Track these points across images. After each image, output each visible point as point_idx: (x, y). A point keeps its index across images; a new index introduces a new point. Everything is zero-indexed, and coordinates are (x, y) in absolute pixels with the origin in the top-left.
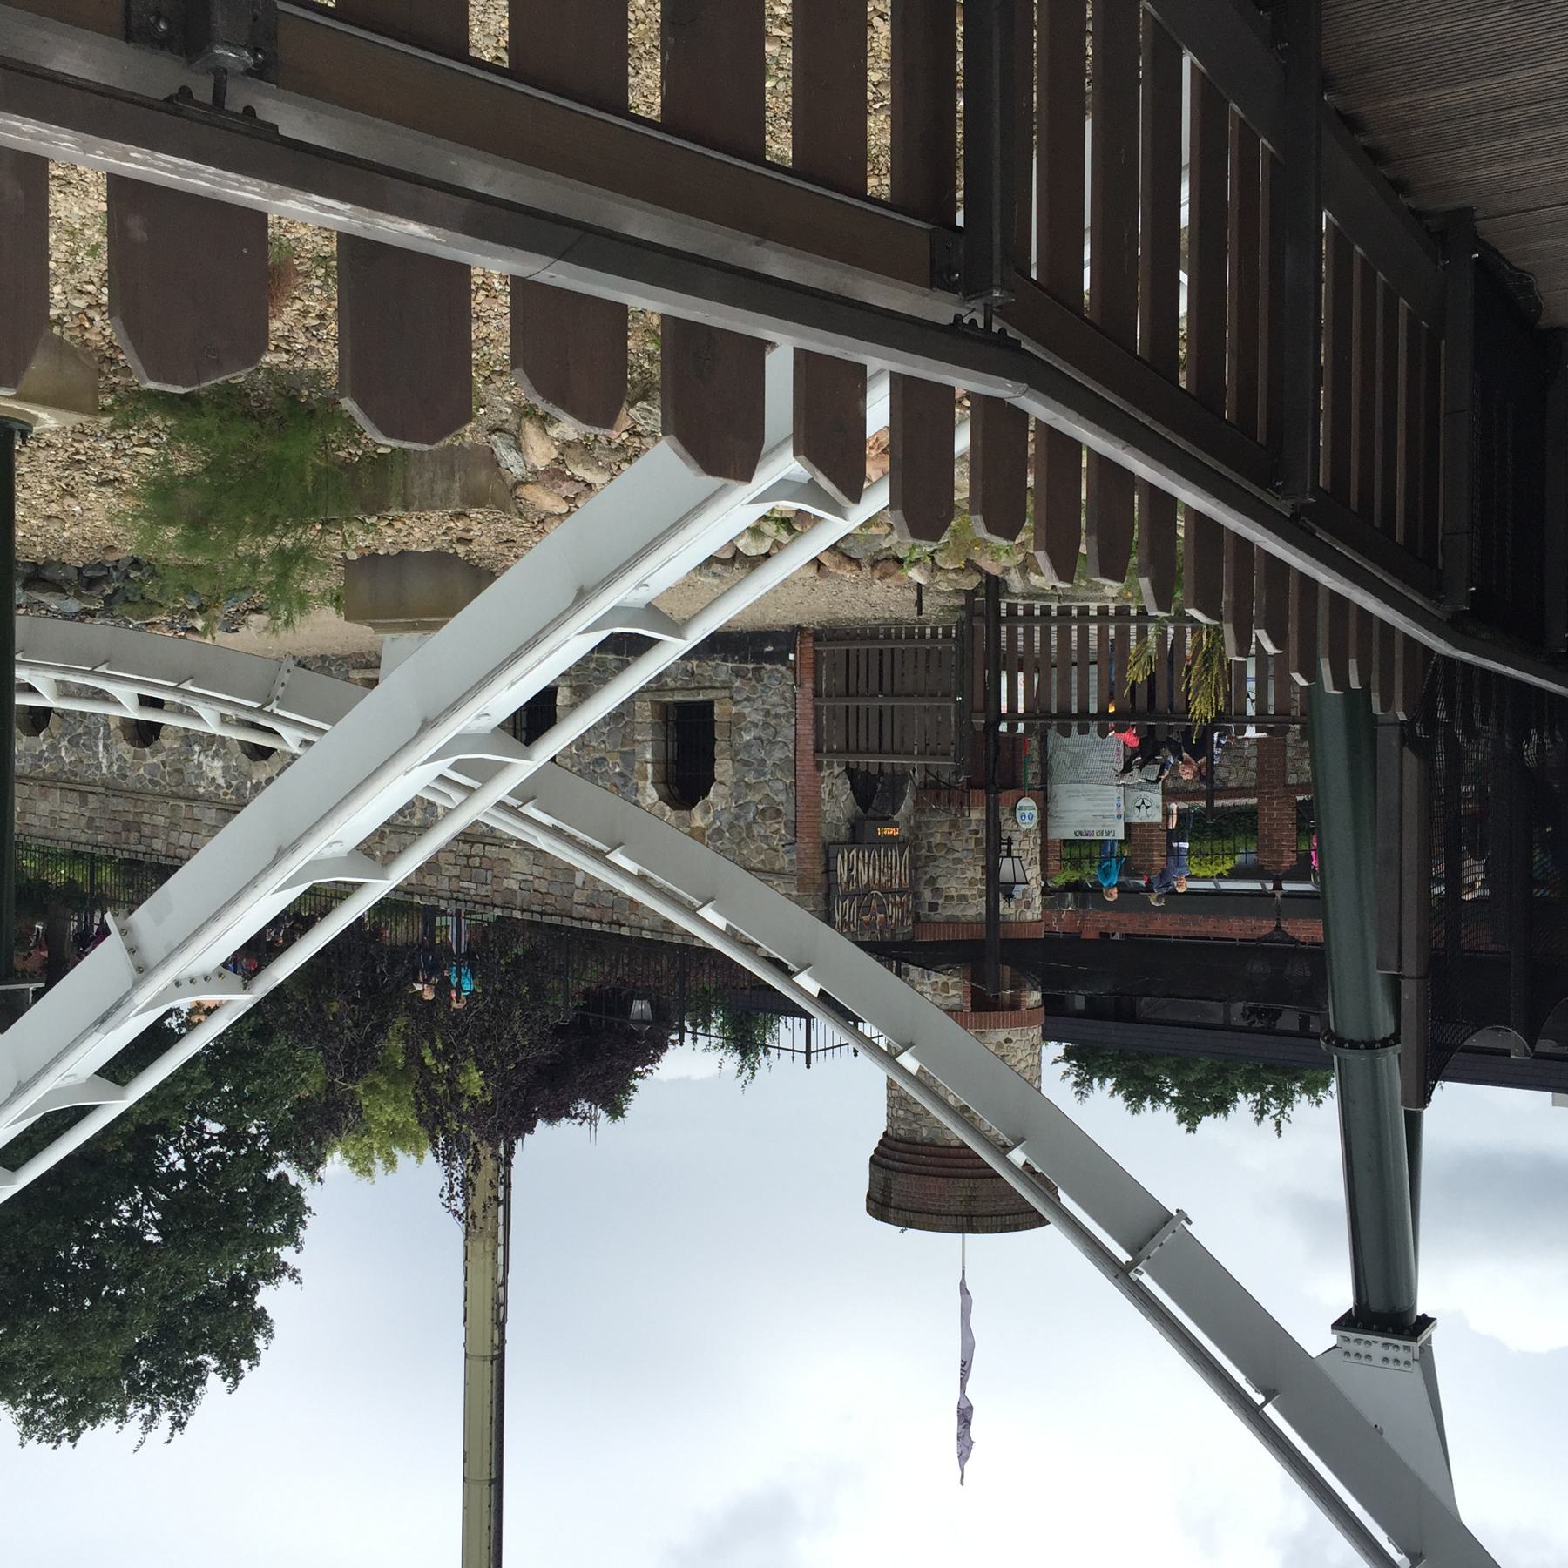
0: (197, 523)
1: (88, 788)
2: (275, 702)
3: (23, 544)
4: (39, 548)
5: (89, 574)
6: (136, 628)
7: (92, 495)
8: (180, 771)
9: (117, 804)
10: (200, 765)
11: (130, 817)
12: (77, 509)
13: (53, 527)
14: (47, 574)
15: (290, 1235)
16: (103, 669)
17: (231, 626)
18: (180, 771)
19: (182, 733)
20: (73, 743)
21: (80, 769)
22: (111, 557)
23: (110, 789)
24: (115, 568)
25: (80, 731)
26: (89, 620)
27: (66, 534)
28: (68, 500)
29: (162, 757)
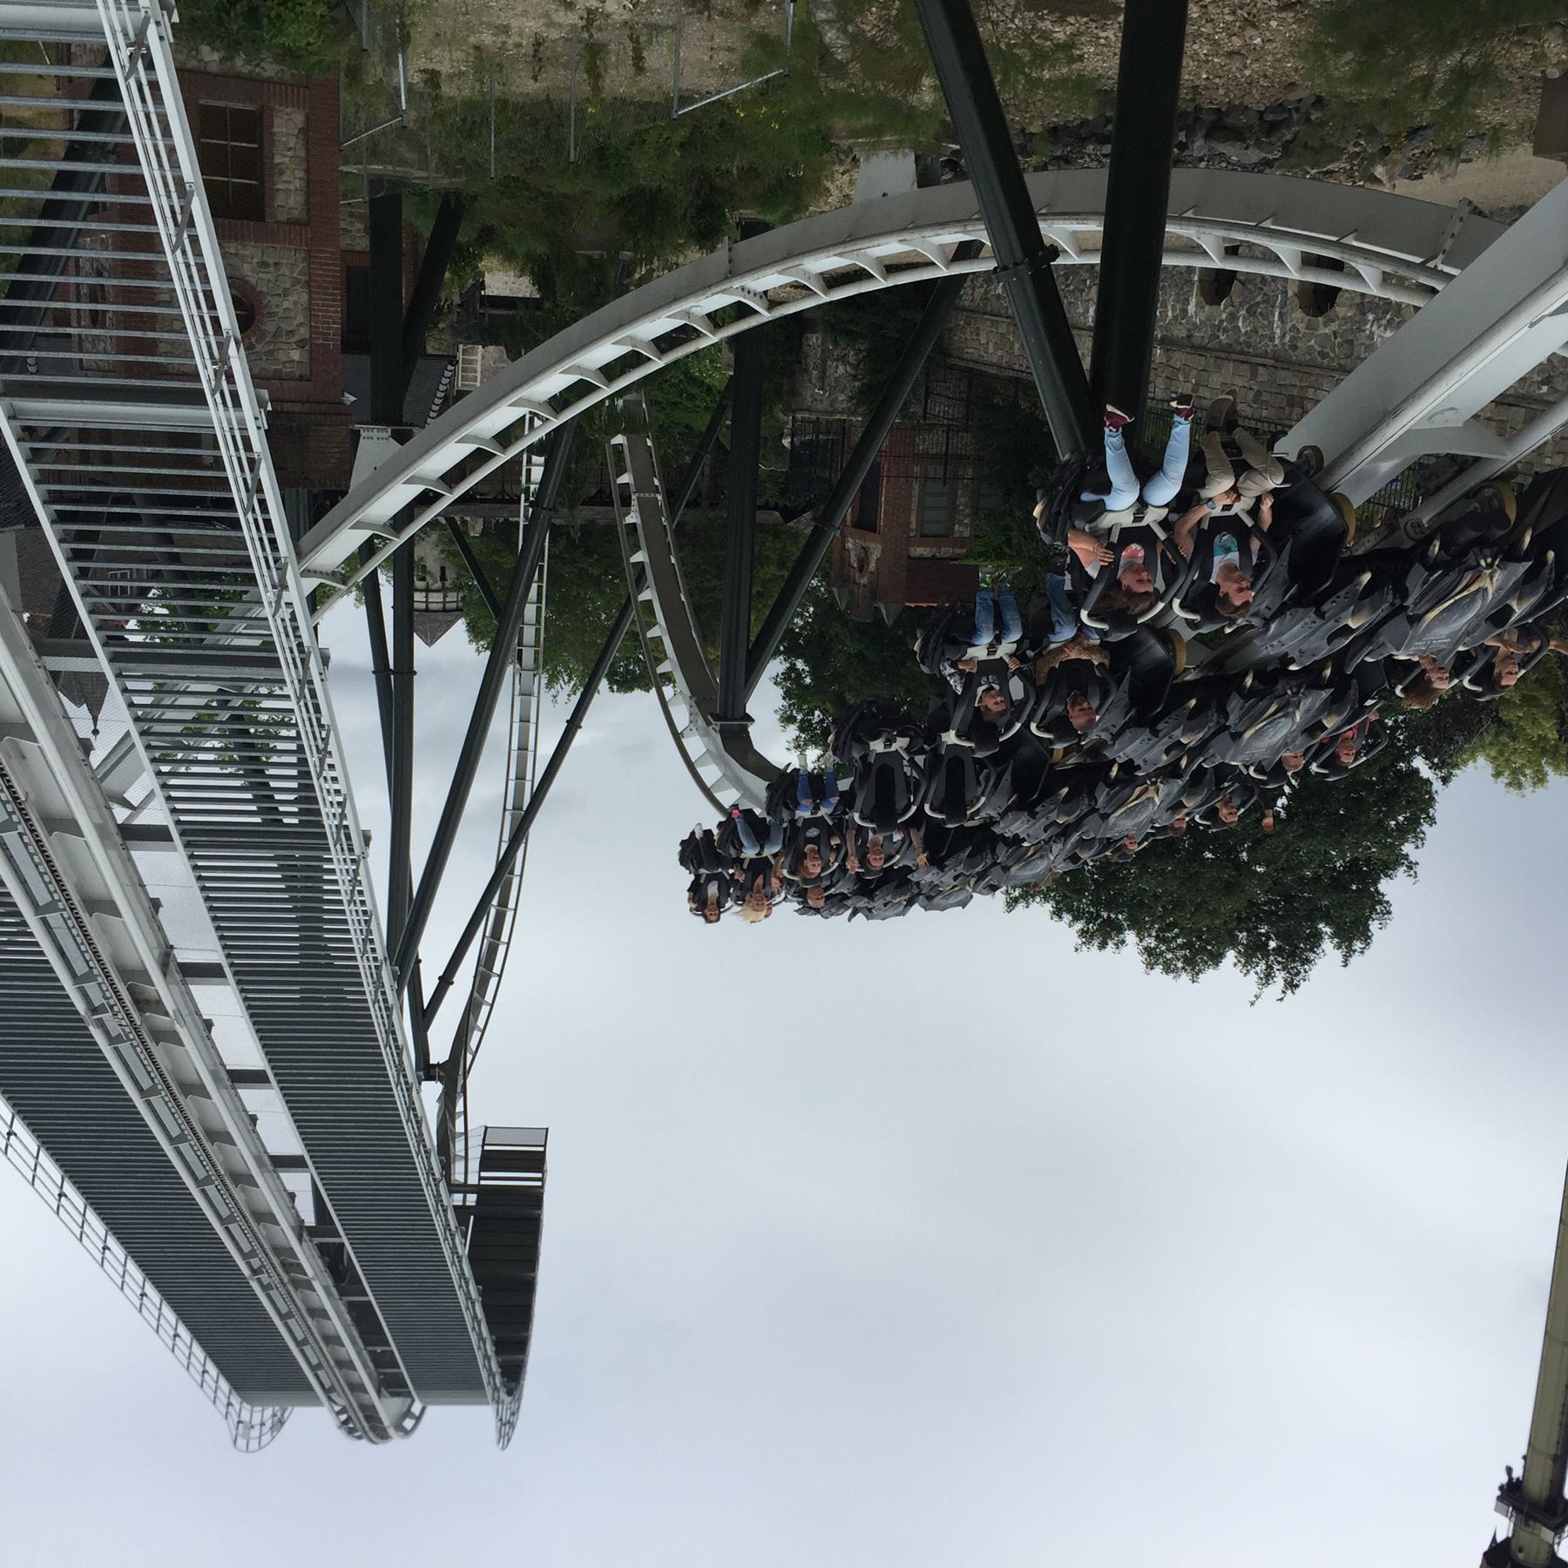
0: (1372, 46)
1: (1260, 360)
2: (1441, 257)
3: (1206, 88)
4: (1221, 92)
5: (1270, 117)
6: (1313, 178)
7: (1274, 24)
8: (1350, 342)
9: (1284, 377)
10: (1372, 333)
11: (1295, 392)
12: (1258, 41)
13: (1235, 65)
14: (1229, 121)
15: (1411, 829)
16: (1268, 224)
17: (1414, 172)
18: (1350, 342)
19: (1358, 300)
20: (1251, 312)
21: (1255, 339)
22: (1293, 97)
23: (1281, 361)
24: (1297, 110)
25: (1259, 299)
26: (1268, 171)
27: (1247, 72)
28: (1250, 32)
29: (1334, 327)
